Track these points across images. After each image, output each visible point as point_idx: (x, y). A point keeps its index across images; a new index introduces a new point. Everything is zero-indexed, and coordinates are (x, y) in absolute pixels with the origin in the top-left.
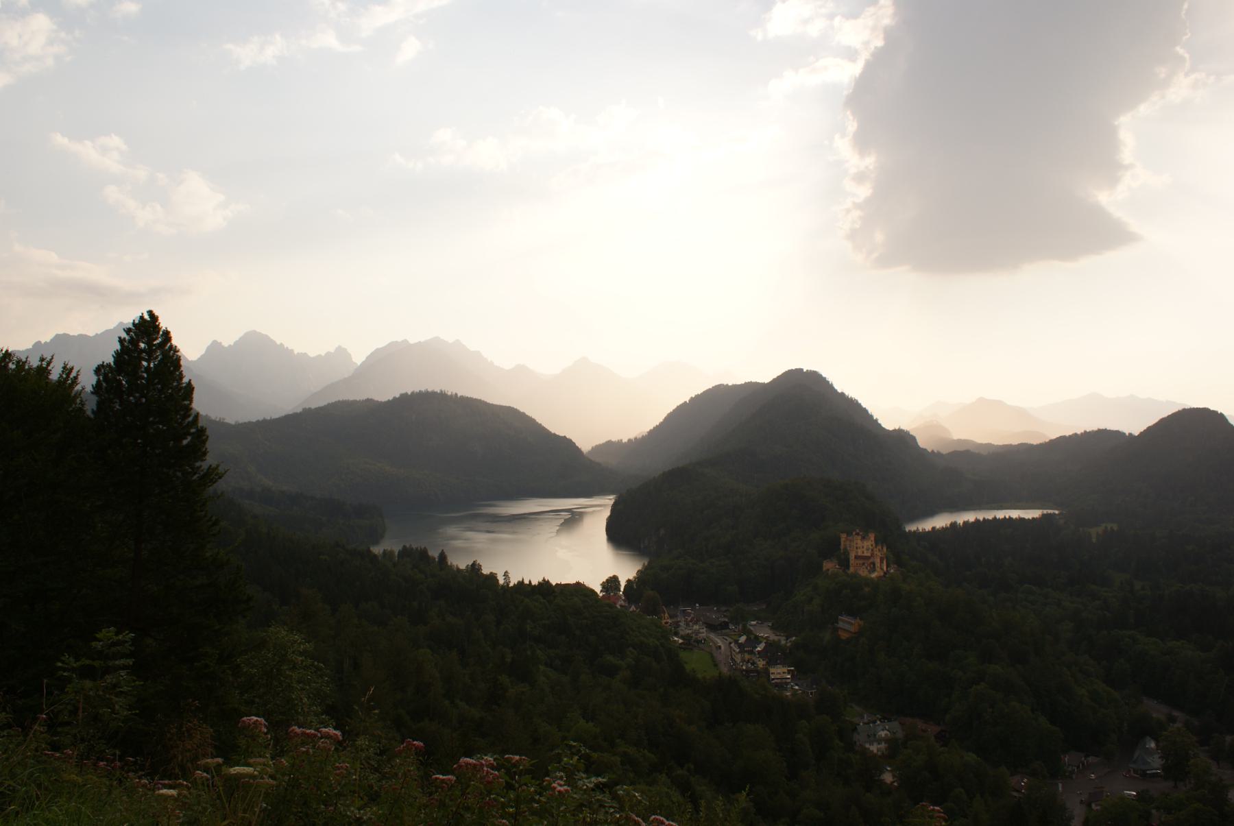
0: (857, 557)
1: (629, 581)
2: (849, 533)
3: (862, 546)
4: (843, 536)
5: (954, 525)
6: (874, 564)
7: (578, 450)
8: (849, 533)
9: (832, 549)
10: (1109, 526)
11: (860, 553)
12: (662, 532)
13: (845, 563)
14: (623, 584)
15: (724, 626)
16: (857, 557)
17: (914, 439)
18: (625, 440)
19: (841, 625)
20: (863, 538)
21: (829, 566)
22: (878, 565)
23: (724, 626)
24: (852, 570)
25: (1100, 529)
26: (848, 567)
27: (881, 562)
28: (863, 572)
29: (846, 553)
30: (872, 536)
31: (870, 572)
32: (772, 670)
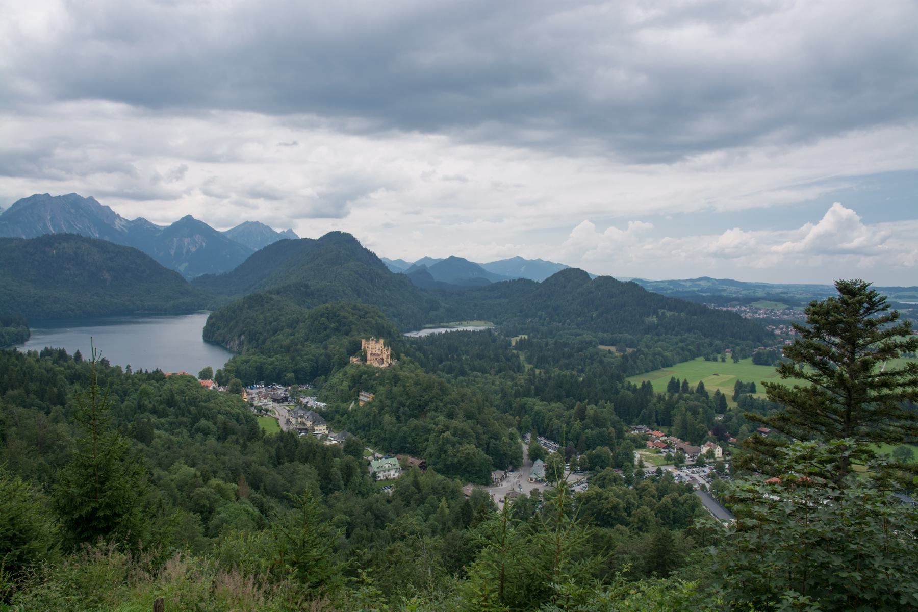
1: (219, 371)
2: (367, 339)
4: (363, 341)
5: (432, 334)
8: (367, 339)
9: (356, 349)
10: (523, 336)
12: (243, 337)
13: (364, 358)
14: (214, 374)
15: (285, 400)
16: (372, 355)
19: (361, 398)
20: (377, 342)
21: (354, 360)
23: (285, 400)
24: (368, 363)
25: (518, 338)
26: (366, 361)
28: (376, 364)
29: (365, 352)
30: (382, 341)
32: (316, 428)
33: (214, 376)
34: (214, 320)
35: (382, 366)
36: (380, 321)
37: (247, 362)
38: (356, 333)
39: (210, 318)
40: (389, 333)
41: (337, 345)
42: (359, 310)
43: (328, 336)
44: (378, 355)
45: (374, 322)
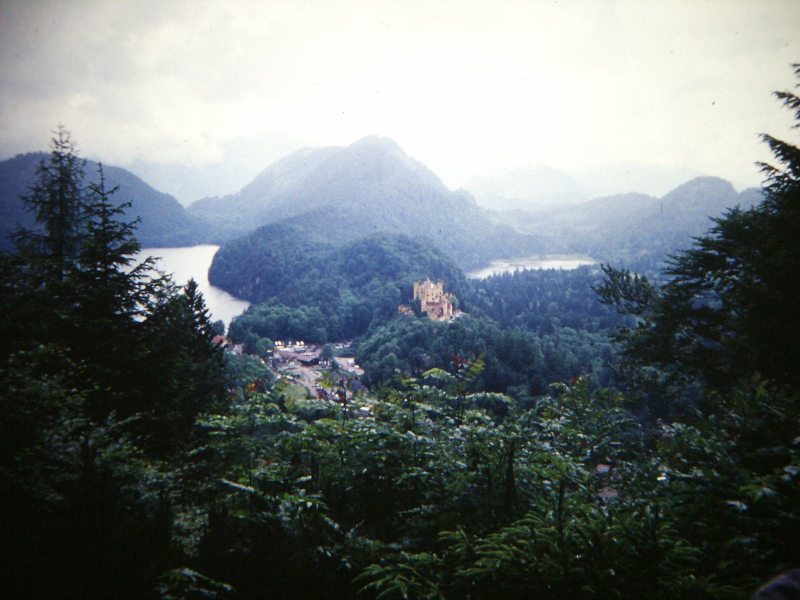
0: (428, 303)
3: (431, 292)
5: (506, 275)
6: (442, 310)
7: (180, 206)
9: (407, 295)
11: (430, 300)
12: (258, 280)
17: (473, 199)
18: (221, 197)
22: (445, 310)
27: (449, 308)
28: (433, 317)
29: (418, 302)
30: (440, 285)
31: (439, 316)
33: (226, 331)
34: (221, 258)
35: (442, 319)
36: (437, 258)
37: (266, 314)
38: (405, 273)
39: (217, 255)
40: (449, 275)
41: (381, 289)
42: (408, 244)
43: (368, 279)
44: (437, 304)
45: (429, 260)
